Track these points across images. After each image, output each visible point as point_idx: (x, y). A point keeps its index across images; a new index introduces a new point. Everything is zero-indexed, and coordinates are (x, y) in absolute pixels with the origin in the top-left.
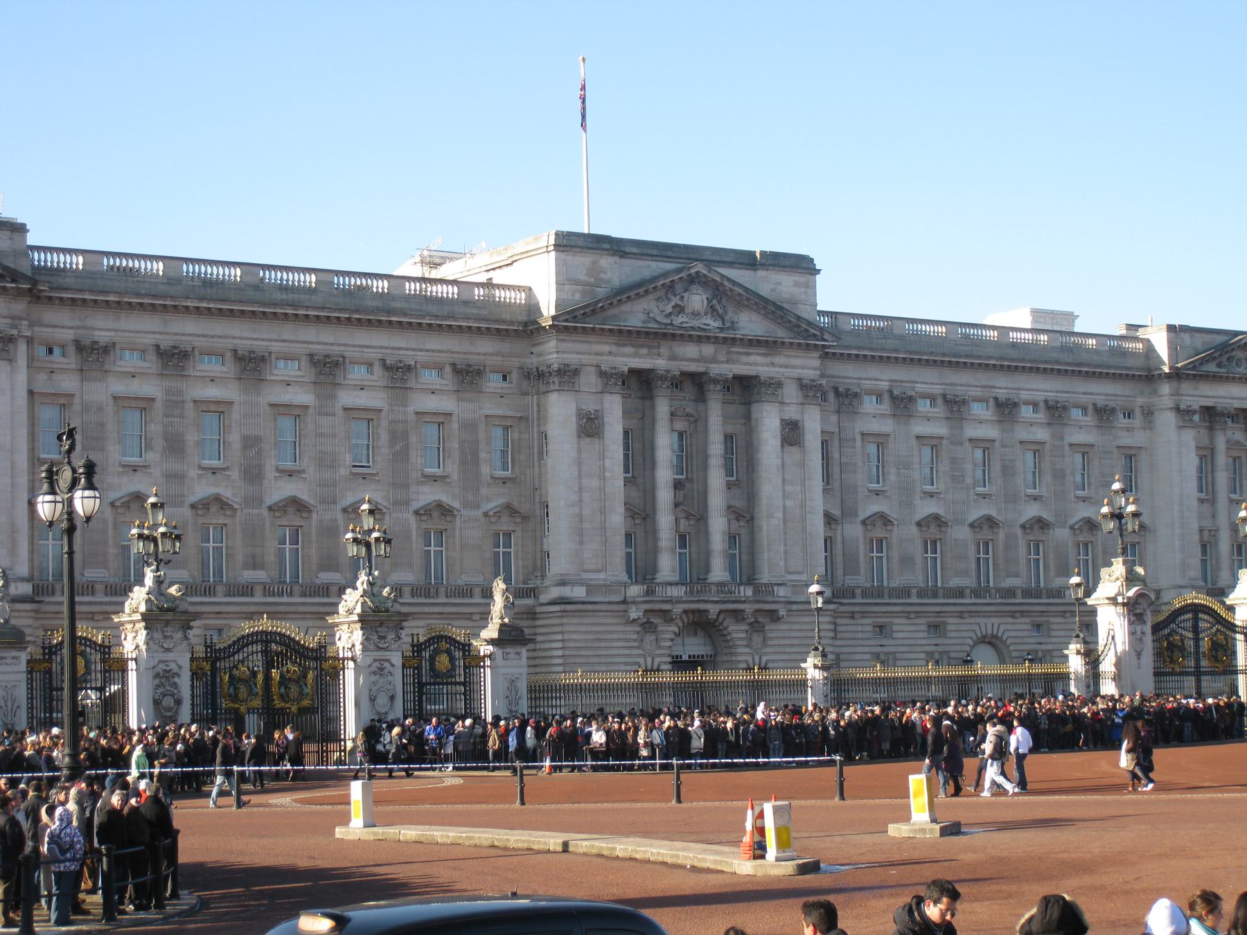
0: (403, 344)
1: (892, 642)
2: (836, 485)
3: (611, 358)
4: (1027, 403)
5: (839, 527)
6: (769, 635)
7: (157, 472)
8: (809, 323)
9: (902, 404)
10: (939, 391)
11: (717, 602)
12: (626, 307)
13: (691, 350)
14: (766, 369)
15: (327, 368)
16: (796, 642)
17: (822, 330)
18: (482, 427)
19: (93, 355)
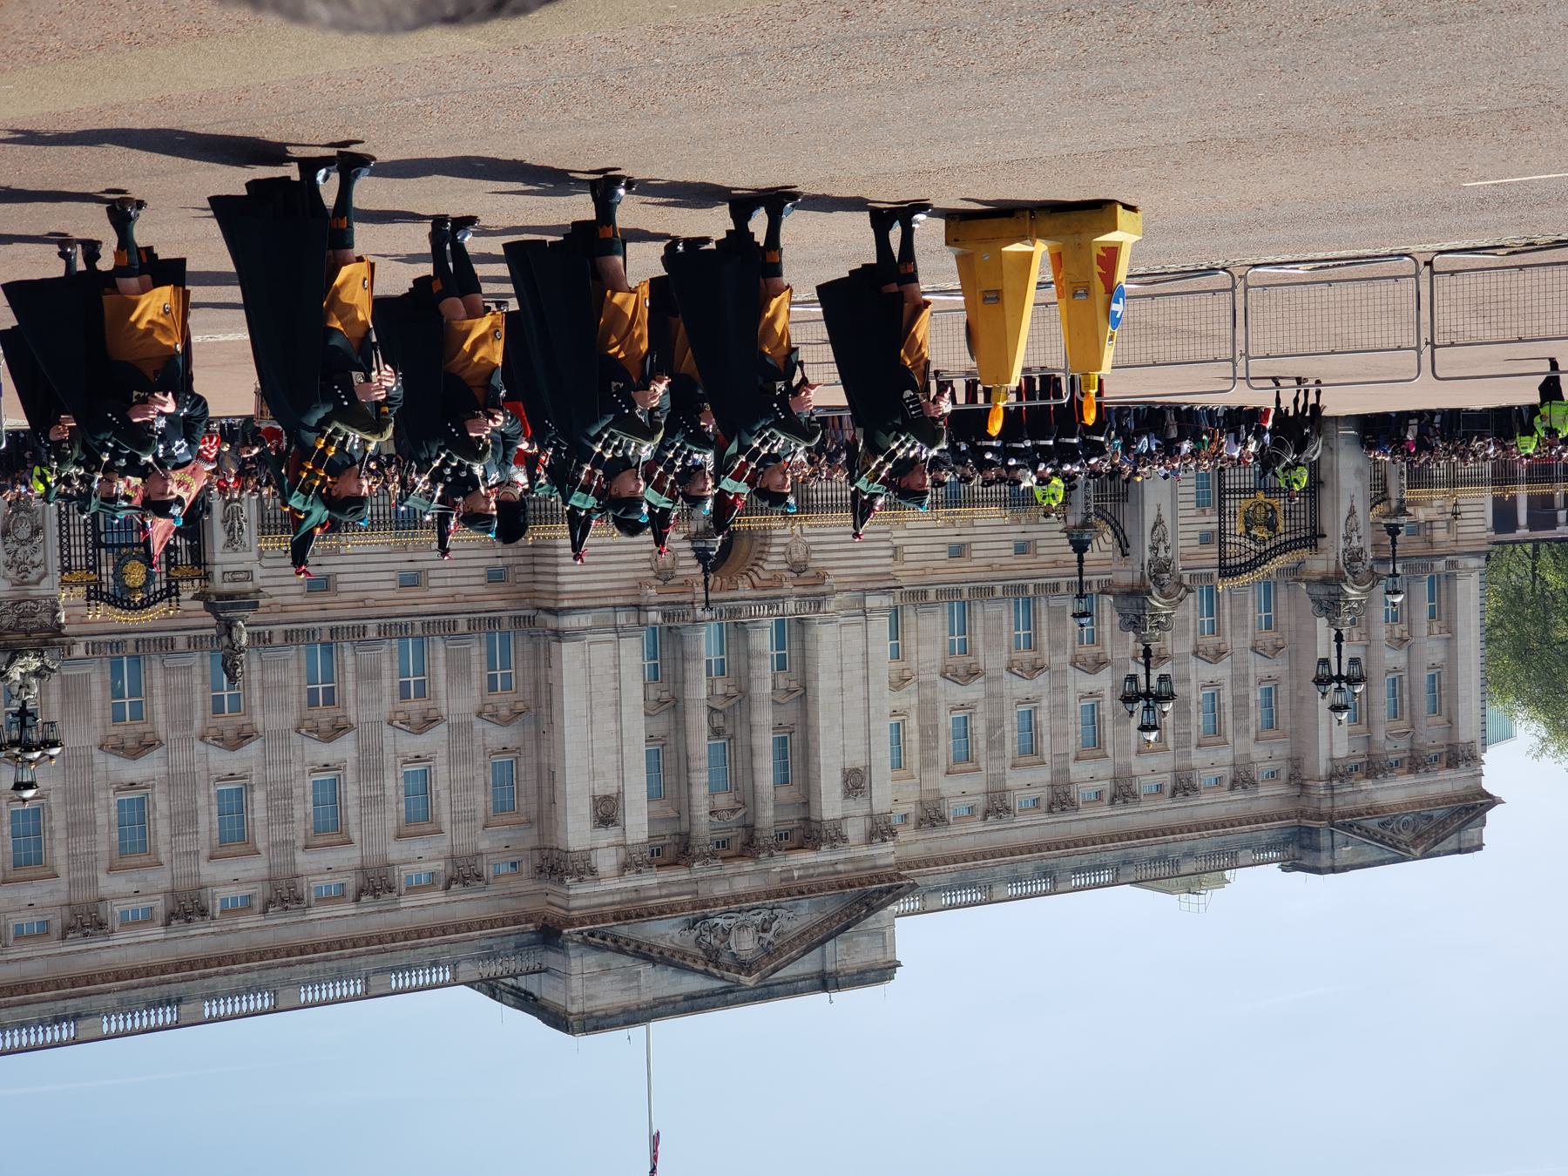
0: (995, 836)
1: (398, 566)
2: (480, 760)
3: (834, 858)
4: (148, 919)
5: (477, 708)
6: (648, 565)
7: (1193, 682)
8: (606, 949)
9: (375, 884)
10: (314, 910)
11: (742, 599)
12: (817, 917)
13: (741, 885)
14: (645, 882)
15: (1060, 801)
16: (612, 558)
17: (585, 943)
18: (916, 766)
19: (1242, 780)
